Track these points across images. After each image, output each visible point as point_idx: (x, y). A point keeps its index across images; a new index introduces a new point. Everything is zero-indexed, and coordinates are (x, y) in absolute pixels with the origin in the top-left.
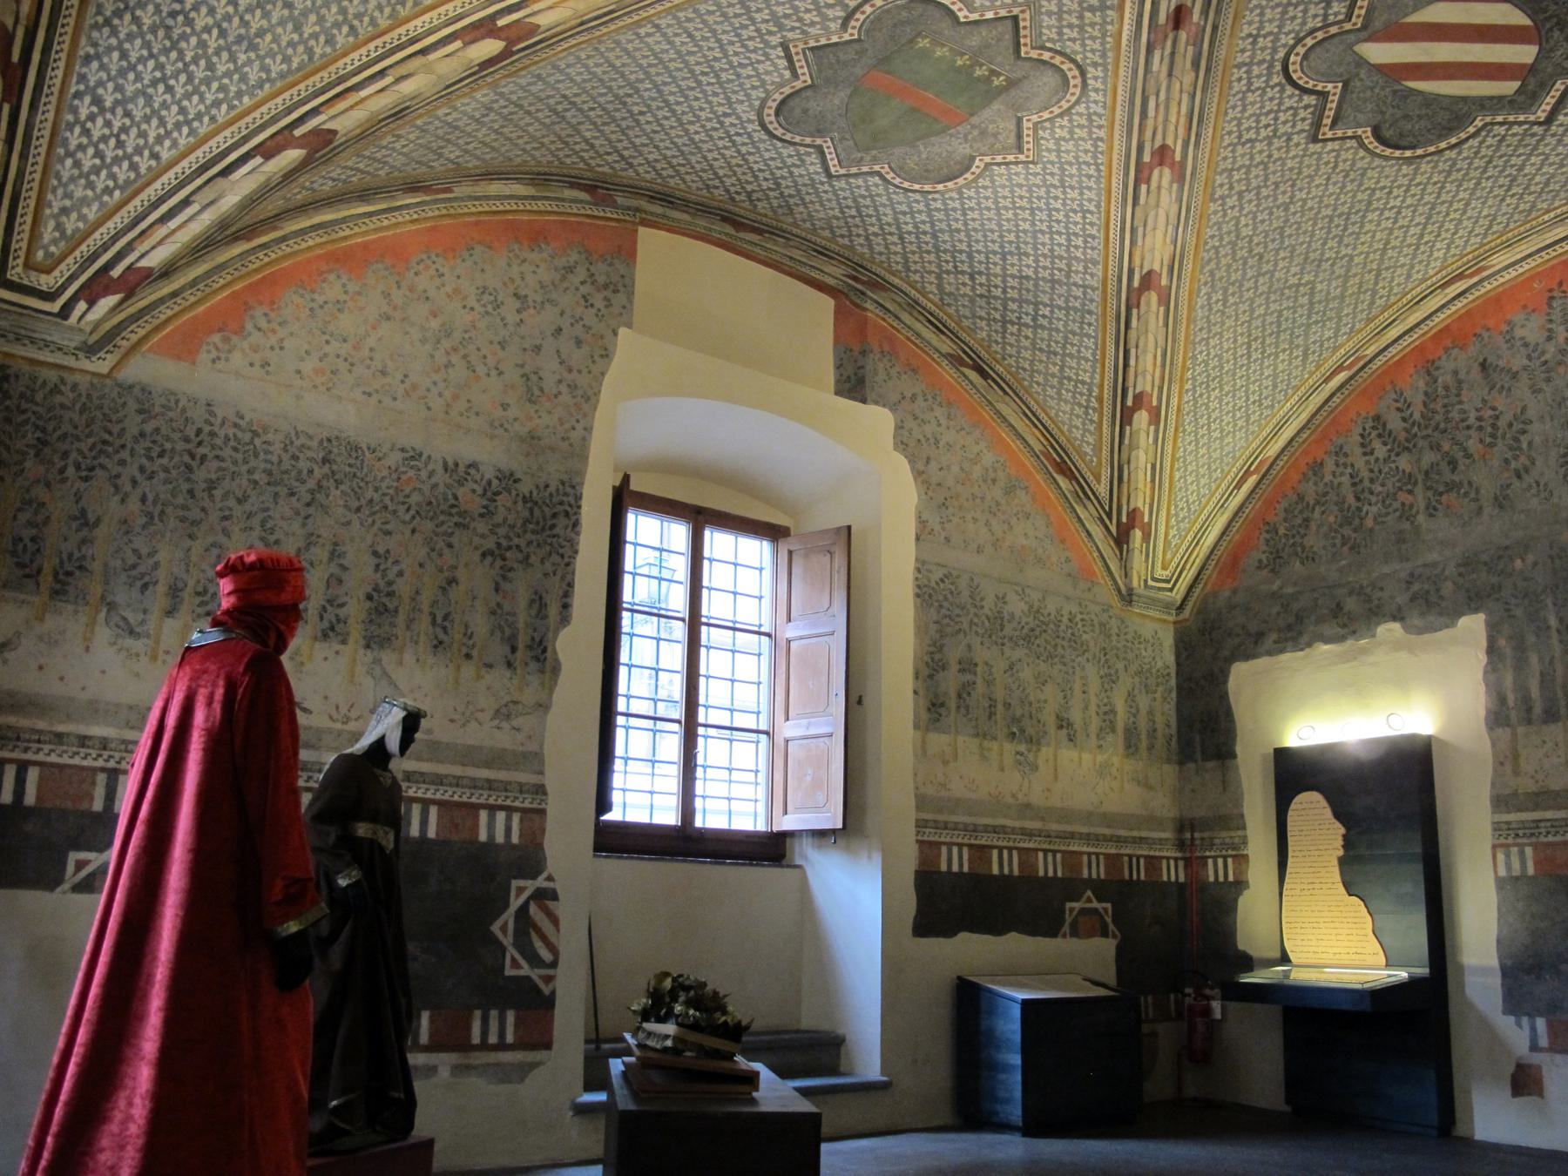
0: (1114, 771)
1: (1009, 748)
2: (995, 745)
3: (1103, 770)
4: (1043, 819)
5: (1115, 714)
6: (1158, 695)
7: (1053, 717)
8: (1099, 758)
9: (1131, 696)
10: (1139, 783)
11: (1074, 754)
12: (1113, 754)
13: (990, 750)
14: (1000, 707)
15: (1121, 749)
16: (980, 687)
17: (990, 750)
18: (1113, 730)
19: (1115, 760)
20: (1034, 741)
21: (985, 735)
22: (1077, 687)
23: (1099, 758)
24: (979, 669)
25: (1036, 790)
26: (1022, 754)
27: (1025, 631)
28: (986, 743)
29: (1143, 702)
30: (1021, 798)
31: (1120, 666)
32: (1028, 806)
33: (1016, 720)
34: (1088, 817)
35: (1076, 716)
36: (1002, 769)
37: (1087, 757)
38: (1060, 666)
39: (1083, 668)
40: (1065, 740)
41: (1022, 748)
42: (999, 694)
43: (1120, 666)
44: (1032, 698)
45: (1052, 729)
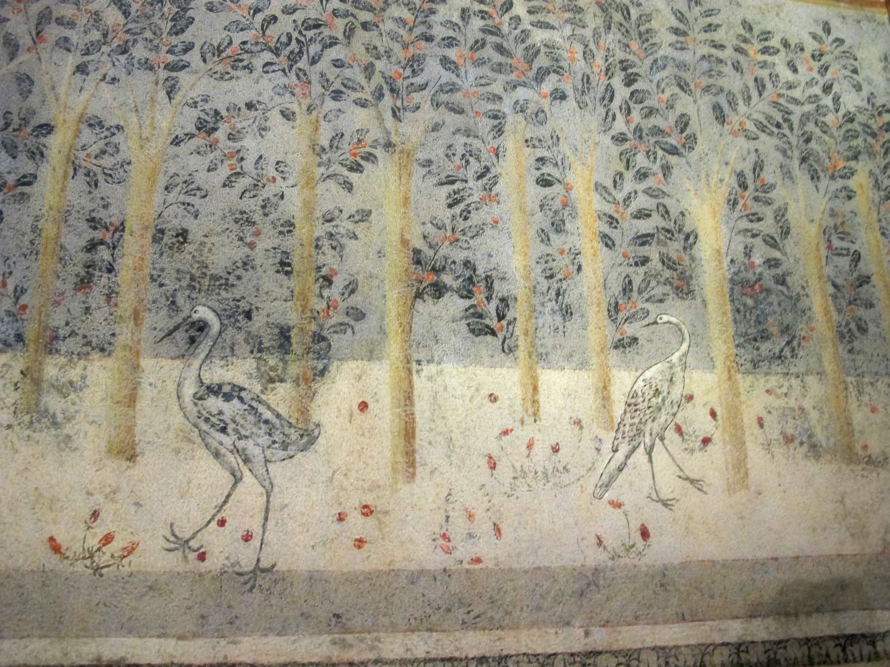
0: (697, 419)
1: (167, 378)
2: (100, 375)
3: (640, 425)
4: (338, 621)
5: (690, 239)
6: (860, 181)
7: (395, 263)
8: (623, 381)
9: (749, 191)
10: (814, 450)
11: (507, 378)
12: (695, 369)
13: (66, 389)
14: (135, 250)
15: (720, 339)
16: (51, 189)
17: (66, 389)
18: (683, 285)
19: (705, 384)
20: (306, 348)
21: (51, 343)
22: (514, 168)
23: (623, 381)
24: (56, 143)
25: (301, 512)
26: (233, 393)
27: (285, 25)
28: (51, 369)
29: (805, 205)
30: (223, 548)
31: (697, 108)
32: (259, 578)
33: (201, 281)
34: (589, 582)
35: (510, 253)
36: (127, 451)
37: (564, 388)
38: (428, 114)
39: (539, 117)
40: (455, 335)
41: (239, 371)
42: (137, 203)
43: (697, 108)
44: (293, 205)
45: (387, 294)
